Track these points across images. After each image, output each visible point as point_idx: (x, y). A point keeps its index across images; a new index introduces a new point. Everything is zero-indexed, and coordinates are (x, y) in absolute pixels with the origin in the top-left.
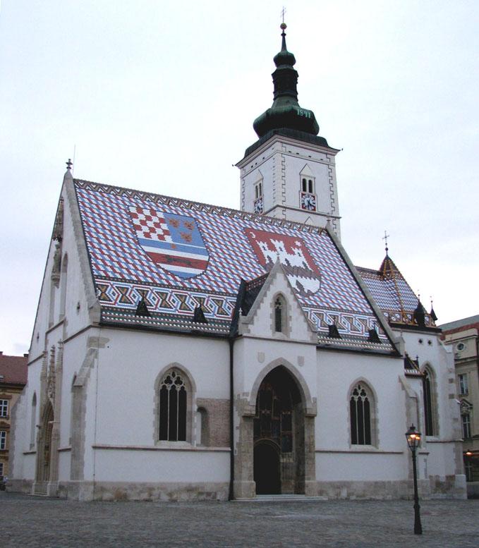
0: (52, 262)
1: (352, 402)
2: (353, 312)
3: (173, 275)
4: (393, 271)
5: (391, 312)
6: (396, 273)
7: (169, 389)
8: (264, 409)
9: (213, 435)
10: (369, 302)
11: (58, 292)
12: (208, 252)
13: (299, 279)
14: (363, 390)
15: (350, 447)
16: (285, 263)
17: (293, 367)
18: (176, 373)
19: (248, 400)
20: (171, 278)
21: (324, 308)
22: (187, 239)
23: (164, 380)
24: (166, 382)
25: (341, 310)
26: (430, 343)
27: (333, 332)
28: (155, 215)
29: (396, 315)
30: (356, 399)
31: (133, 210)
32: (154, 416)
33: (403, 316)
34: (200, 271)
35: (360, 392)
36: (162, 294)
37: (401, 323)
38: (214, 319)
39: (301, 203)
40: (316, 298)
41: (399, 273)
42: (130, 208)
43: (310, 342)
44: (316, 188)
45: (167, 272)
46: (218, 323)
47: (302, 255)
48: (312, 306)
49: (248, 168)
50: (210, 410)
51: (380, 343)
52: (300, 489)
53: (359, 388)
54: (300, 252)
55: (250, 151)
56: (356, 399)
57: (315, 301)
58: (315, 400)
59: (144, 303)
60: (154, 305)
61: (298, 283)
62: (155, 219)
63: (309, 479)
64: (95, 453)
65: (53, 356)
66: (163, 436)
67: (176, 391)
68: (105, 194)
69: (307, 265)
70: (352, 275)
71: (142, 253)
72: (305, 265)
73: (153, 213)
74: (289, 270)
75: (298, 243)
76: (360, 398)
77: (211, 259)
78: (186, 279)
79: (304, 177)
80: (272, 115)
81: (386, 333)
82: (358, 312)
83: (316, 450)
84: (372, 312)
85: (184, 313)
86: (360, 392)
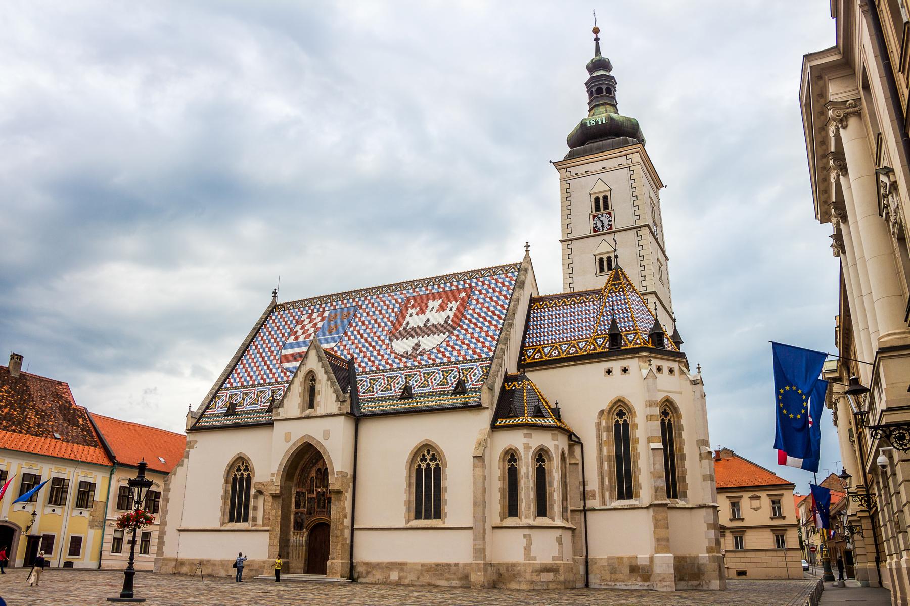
1: (419, 470)
4: (624, 282)
5: (574, 342)
6: (615, 285)
7: (238, 477)
14: (433, 455)
15: (408, 521)
17: (318, 442)
23: (235, 469)
26: (625, 370)
35: (428, 457)
40: (425, 357)
44: (614, 203)
45: (283, 368)
50: (264, 491)
53: (428, 453)
57: (419, 361)
63: (333, 558)
66: (231, 520)
71: (277, 357)
74: (428, 330)
75: (463, 295)
76: (428, 465)
79: (596, 195)
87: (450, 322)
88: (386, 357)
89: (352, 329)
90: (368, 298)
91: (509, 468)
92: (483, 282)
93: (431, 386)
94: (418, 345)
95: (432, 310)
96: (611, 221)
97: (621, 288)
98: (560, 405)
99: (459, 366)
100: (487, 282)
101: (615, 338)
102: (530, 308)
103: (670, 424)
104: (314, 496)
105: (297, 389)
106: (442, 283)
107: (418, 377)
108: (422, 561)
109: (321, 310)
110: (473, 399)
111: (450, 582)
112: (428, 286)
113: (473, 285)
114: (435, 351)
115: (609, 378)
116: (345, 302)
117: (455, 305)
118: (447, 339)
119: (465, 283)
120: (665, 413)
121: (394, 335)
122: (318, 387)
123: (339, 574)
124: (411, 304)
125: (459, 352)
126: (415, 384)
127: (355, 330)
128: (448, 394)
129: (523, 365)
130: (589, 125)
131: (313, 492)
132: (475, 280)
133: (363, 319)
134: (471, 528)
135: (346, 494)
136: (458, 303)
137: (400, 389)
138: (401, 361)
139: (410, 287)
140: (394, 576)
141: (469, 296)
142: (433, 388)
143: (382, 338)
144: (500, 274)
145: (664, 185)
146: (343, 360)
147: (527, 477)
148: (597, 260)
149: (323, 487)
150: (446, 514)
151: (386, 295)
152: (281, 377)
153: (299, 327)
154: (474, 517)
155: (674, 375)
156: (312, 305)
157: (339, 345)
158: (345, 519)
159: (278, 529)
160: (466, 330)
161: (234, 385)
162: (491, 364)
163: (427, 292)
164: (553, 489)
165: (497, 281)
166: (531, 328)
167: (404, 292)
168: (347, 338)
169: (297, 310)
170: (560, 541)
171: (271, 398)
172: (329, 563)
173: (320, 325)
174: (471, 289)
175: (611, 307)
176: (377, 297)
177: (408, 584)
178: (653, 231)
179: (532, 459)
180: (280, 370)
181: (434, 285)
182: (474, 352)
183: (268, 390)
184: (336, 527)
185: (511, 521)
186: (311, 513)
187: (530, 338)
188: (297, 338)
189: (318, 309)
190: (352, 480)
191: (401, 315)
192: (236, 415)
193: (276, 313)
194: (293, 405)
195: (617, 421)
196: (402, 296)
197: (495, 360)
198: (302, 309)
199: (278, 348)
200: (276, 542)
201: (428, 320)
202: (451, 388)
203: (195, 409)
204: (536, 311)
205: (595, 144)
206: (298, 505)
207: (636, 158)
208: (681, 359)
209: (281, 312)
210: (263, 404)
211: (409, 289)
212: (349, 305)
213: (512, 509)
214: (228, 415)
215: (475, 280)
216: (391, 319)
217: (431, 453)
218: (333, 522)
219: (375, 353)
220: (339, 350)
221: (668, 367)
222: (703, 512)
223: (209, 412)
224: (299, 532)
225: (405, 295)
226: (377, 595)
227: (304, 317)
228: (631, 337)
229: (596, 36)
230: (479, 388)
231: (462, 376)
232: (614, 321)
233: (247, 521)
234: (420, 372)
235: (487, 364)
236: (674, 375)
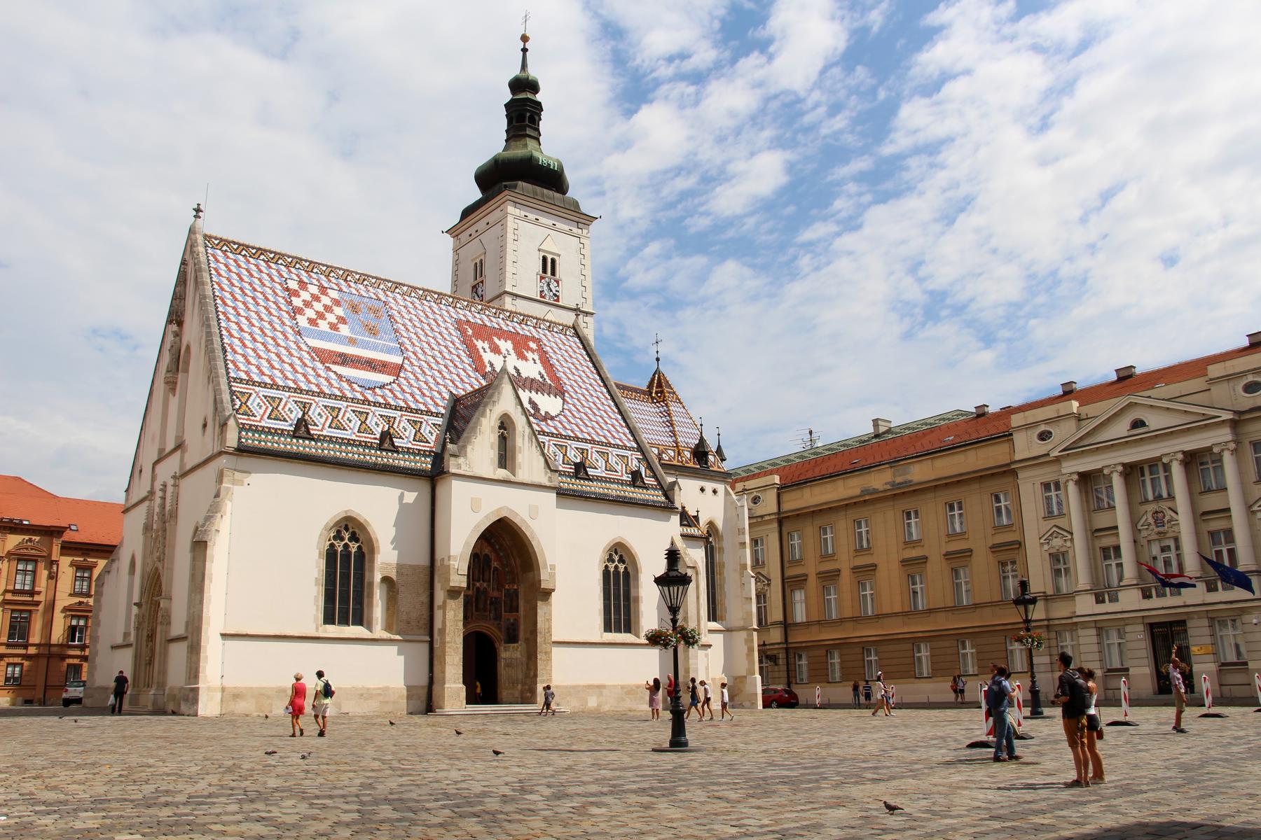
0: (167, 358)
1: (606, 573)
2: (609, 445)
3: (349, 382)
4: (666, 390)
5: (661, 448)
6: (669, 393)
8: (478, 581)
9: (404, 617)
10: (631, 432)
11: (174, 402)
12: (402, 350)
13: (534, 395)
14: (621, 557)
15: (602, 637)
16: (513, 372)
18: (350, 527)
20: (347, 387)
21: (569, 438)
22: (373, 332)
24: (335, 538)
25: (592, 441)
26: (715, 492)
27: (580, 470)
28: (326, 295)
29: (669, 451)
31: (293, 285)
32: (316, 588)
33: (679, 454)
34: (391, 379)
36: (333, 408)
37: (675, 463)
38: (408, 448)
39: (539, 289)
40: (557, 423)
41: (674, 393)
42: (288, 281)
43: (548, 484)
45: (340, 377)
46: (414, 454)
47: (538, 361)
48: (552, 435)
49: (464, 237)
51: (647, 488)
52: (527, 697)
54: (536, 357)
55: (467, 213)
58: (553, 567)
59: (305, 421)
60: (320, 423)
61: (531, 402)
62: (326, 300)
65: (164, 498)
66: (329, 619)
67: (350, 552)
68: (251, 259)
69: (545, 377)
70: (609, 391)
72: (542, 377)
73: (323, 290)
75: (533, 345)
76: (616, 567)
77: (406, 361)
78: (369, 389)
81: (655, 476)
82: (617, 446)
83: (554, 639)
84: (635, 446)
85: (365, 437)
86: (616, 558)
101: (700, 452)
130: (540, 163)
140: (592, 703)
149: (484, 581)
153: (297, 302)
173: (339, 311)
180: (332, 374)
192: (313, 439)
205: (545, 191)
214: (304, 438)
217: (619, 554)
218: (541, 633)
228: (711, 458)
229: (524, 45)
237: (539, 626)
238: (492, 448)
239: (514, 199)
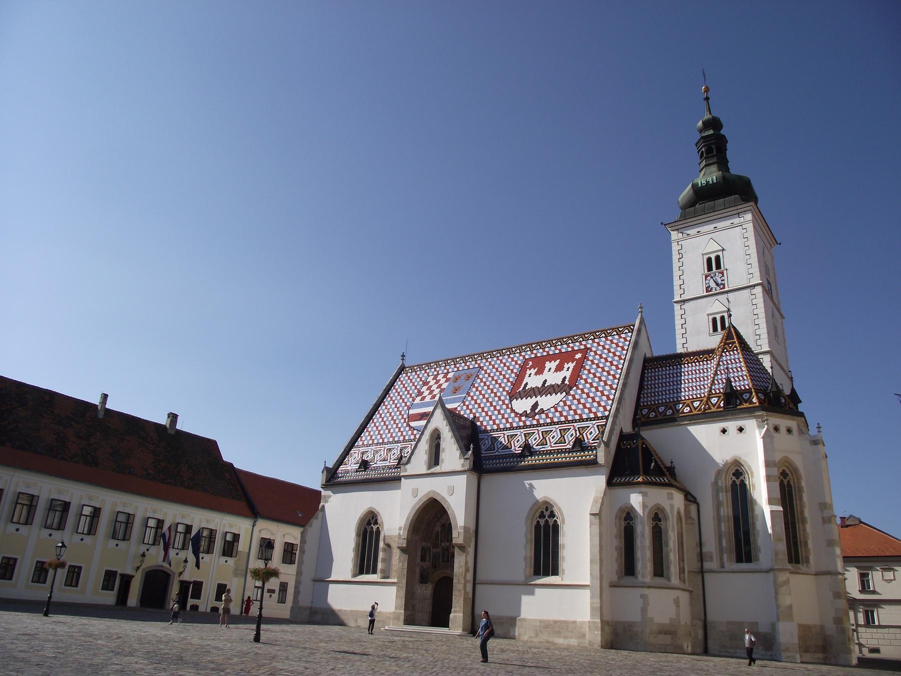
6: (728, 344)
8: (444, 542)
19: (401, 534)
25: (567, 421)
30: (542, 523)
35: (547, 514)
44: (726, 263)
48: (530, 426)
50: (394, 545)
53: (547, 509)
56: (542, 523)
57: (538, 420)
63: (455, 612)
64: (314, 585)
69: (567, 380)
71: (405, 416)
74: (546, 390)
75: (578, 356)
76: (547, 521)
80: (681, 200)
86: (547, 514)
87: (567, 382)
88: (506, 416)
89: (474, 389)
90: (489, 360)
91: (625, 528)
92: (598, 344)
93: (549, 444)
94: (536, 405)
95: (549, 371)
96: (724, 280)
97: (736, 347)
98: (675, 464)
99: (575, 424)
100: (602, 343)
102: (644, 368)
103: (789, 485)
104: (438, 550)
105: (424, 446)
106: (559, 345)
107: (537, 436)
108: (540, 618)
109: (445, 371)
110: (588, 456)
111: (567, 640)
112: (545, 348)
113: (589, 346)
114: (553, 410)
115: (724, 436)
116: (468, 364)
117: (571, 365)
118: (564, 399)
119: (581, 344)
120: (784, 474)
121: (513, 395)
122: (443, 445)
123: (461, 628)
124: (530, 365)
125: (575, 411)
126: (534, 442)
127: (477, 390)
128: (565, 452)
129: (635, 423)
130: (700, 185)
131: (438, 547)
132: (590, 342)
133: (484, 380)
134: (588, 586)
135: (469, 549)
136: (574, 364)
137: (520, 447)
138: (520, 420)
139: (528, 349)
141: (585, 358)
142: (551, 446)
143: (502, 398)
144: (614, 335)
145: (779, 243)
146: (466, 419)
147: (643, 536)
148: (711, 320)
149: (447, 542)
150: (563, 571)
151: (506, 357)
152: (409, 435)
154: (591, 574)
155: (793, 435)
156: (437, 367)
157: (462, 404)
158: (468, 574)
159: (404, 581)
160: (582, 390)
161: (366, 443)
162: (606, 423)
163: (545, 354)
164: (669, 548)
165: (612, 341)
166: (646, 387)
167: (523, 354)
168: (469, 398)
169: (423, 372)
170: (677, 602)
171: (400, 456)
172: (451, 616)
173: (445, 386)
174: (586, 350)
175: (725, 366)
176: (498, 359)
177: (527, 641)
178: (767, 289)
179: (647, 518)
180: (407, 429)
181: (551, 346)
182: (590, 411)
183: (396, 447)
184: (459, 579)
185: (629, 580)
186: (435, 567)
187: (644, 397)
188: (423, 398)
189: (443, 371)
190: (474, 535)
191: (520, 376)
193: (404, 375)
194: (419, 462)
195: (734, 482)
196: (521, 358)
197: (610, 419)
198: (428, 371)
199: (406, 408)
200: (403, 593)
201: (545, 381)
202: (568, 447)
203: (330, 465)
204: (650, 371)
206: (423, 559)
207: (749, 217)
208: (799, 418)
209: (409, 374)
210: (393, 462)
211: (527, 351)
212: (471, 367)
213: (629, 567)
215: (590, 342)
216: (511, 380)
217: (549, 510)
219: (496, 412)
220: (462, 409)
221: (786, 426)
222: (829, 577)
223: (342, 468)
224: (424, 585)
225: (524, 357)
226: (496, 649)
227: (430, 379)
230: (595, 446)
231: (578, 434)
232: (728, 380)
233: (376, 574)
234: (538, 431)
235: (603, 422)
236: (793, 435)
237: (455, 571)
238: (426, 454)
239: (677, 227)
